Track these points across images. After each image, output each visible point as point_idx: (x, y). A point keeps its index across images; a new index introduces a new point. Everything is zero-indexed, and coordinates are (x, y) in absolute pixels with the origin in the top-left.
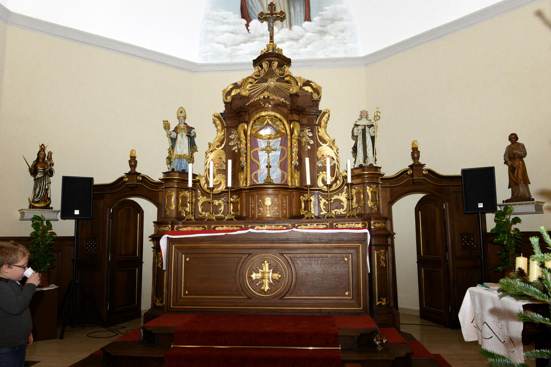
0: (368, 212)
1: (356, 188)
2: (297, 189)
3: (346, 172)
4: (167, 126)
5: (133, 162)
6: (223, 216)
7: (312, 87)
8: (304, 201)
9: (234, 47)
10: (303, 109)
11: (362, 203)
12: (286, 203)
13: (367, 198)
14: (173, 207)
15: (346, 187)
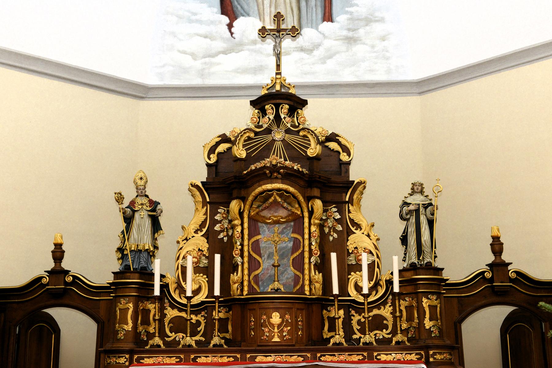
1: (407, 299)
3: (392, 274)
4: (119, 198)
5: (58, 253)
6: (204, 339)
7: (339, 143)
9: (207, 60)
10: (326, 178)
12: (302, 321)
14: (129, 327)
15: (391, 297)
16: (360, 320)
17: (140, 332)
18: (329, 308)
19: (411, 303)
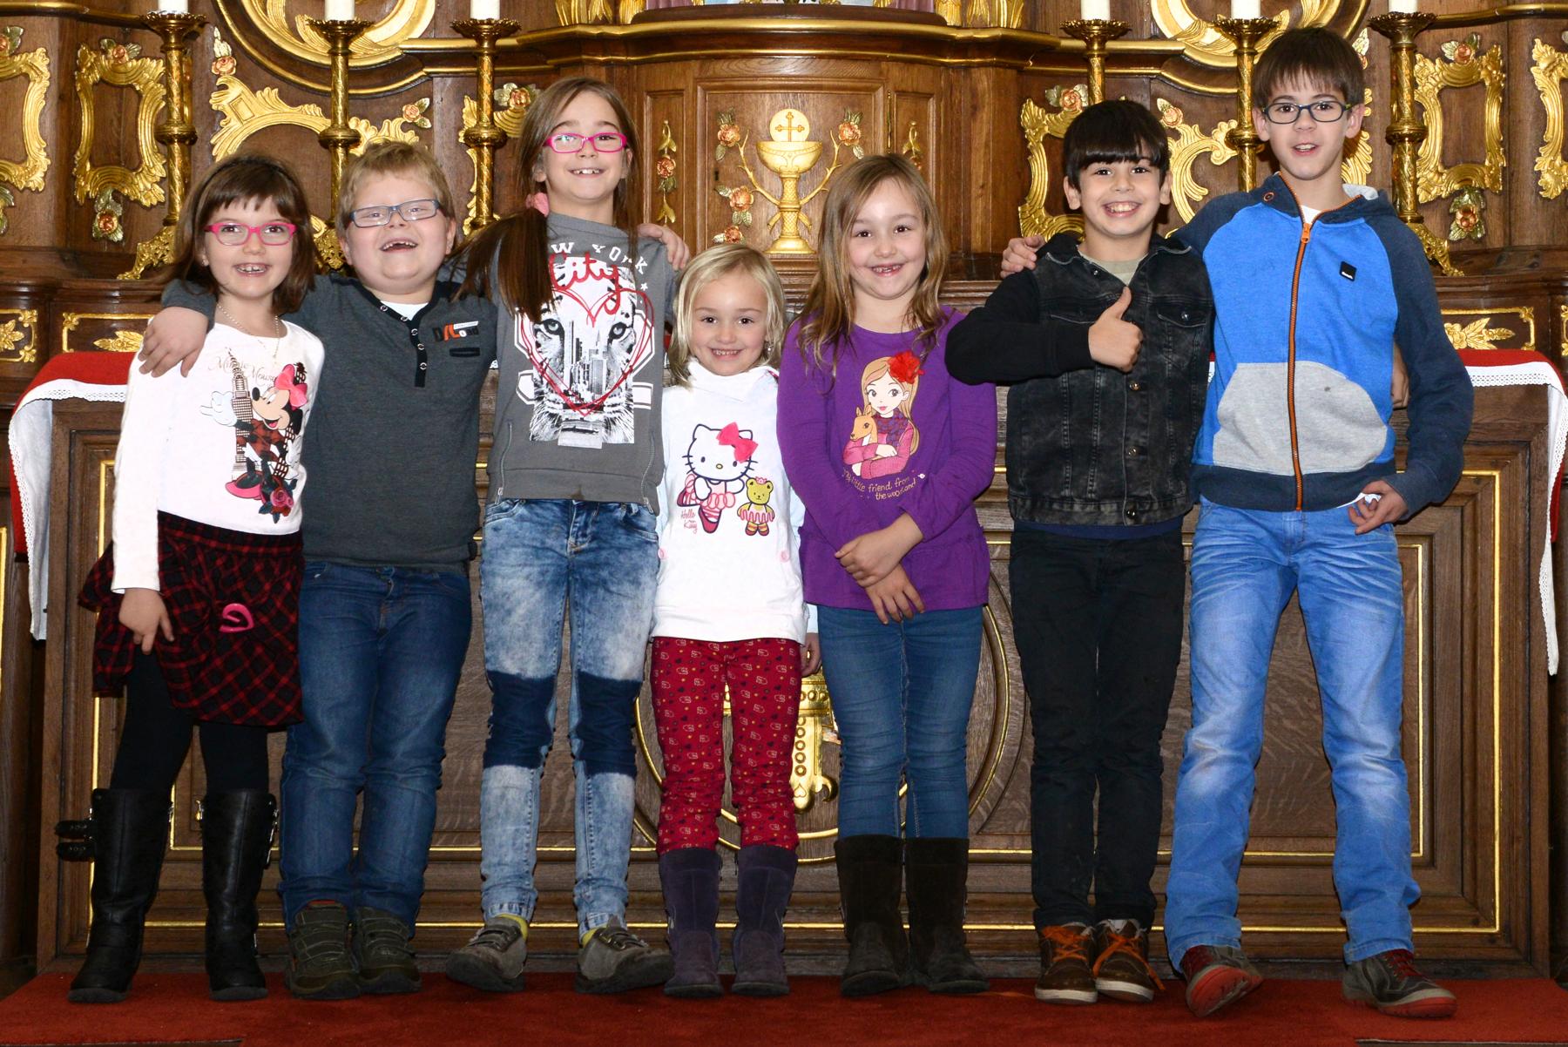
0: (1533, 231)
1: (1449, 49)
2: (1005, 49)
8: (1049, 140)
11: (1493, 161)
13: (1528, 131)
16: (1206, 156)
17: (90, 202)
18: (1053, 94)
19: (1472, 70)
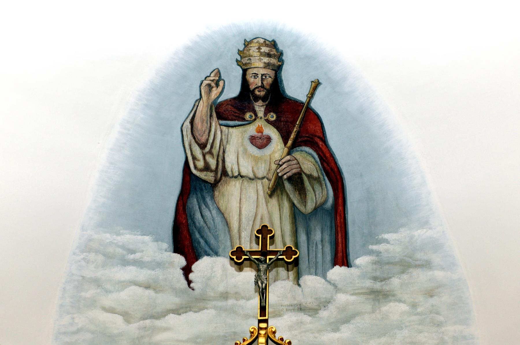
9: (148, 322)
